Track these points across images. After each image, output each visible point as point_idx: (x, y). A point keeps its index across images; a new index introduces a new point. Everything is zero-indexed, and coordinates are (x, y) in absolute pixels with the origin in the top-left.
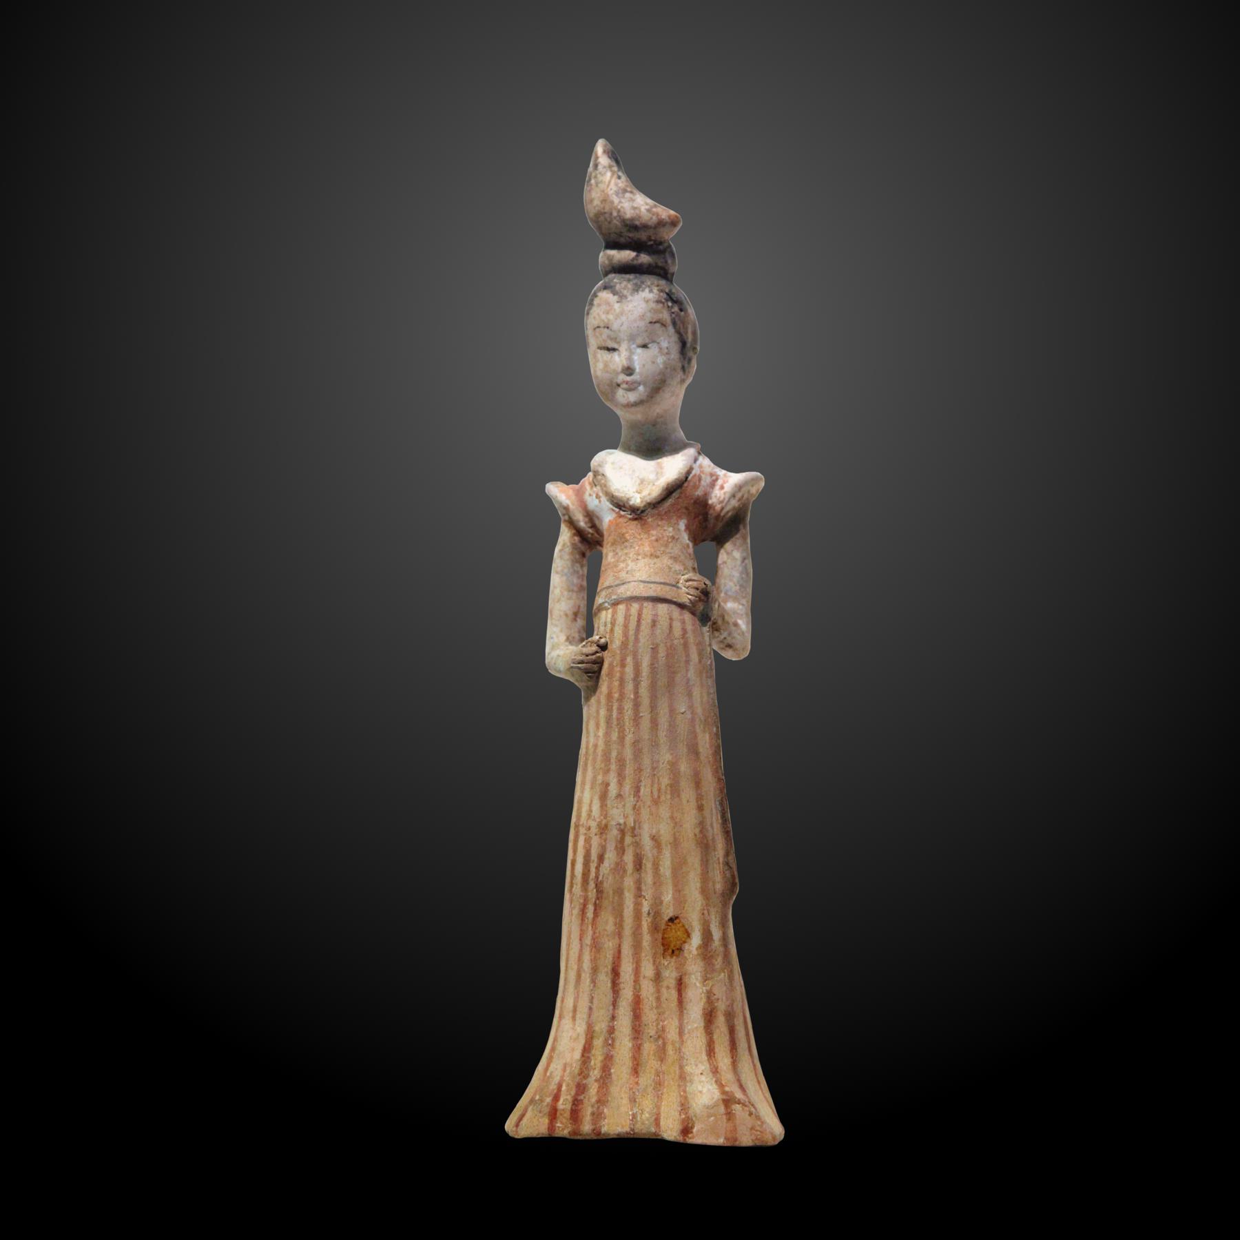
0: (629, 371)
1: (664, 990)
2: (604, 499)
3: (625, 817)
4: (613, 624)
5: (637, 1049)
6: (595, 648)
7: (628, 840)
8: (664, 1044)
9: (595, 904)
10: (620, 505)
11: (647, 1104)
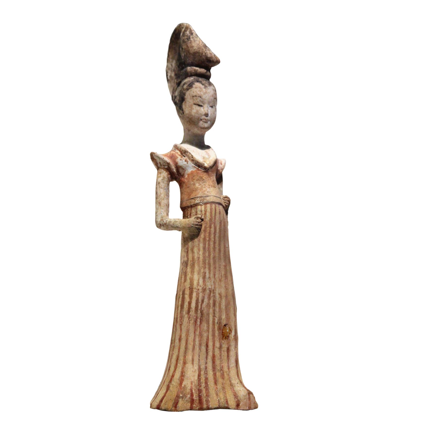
0: (207, 115)
1: (222, 352)
2: (190, 162)
3: (211, 286)
4: (206, 211)
5: (215, 375)
6: (200, 220)
7: (212, 295)
8: (223, 372)
9: (200, 319)
10: (199, 165)
11: (221, 395)
